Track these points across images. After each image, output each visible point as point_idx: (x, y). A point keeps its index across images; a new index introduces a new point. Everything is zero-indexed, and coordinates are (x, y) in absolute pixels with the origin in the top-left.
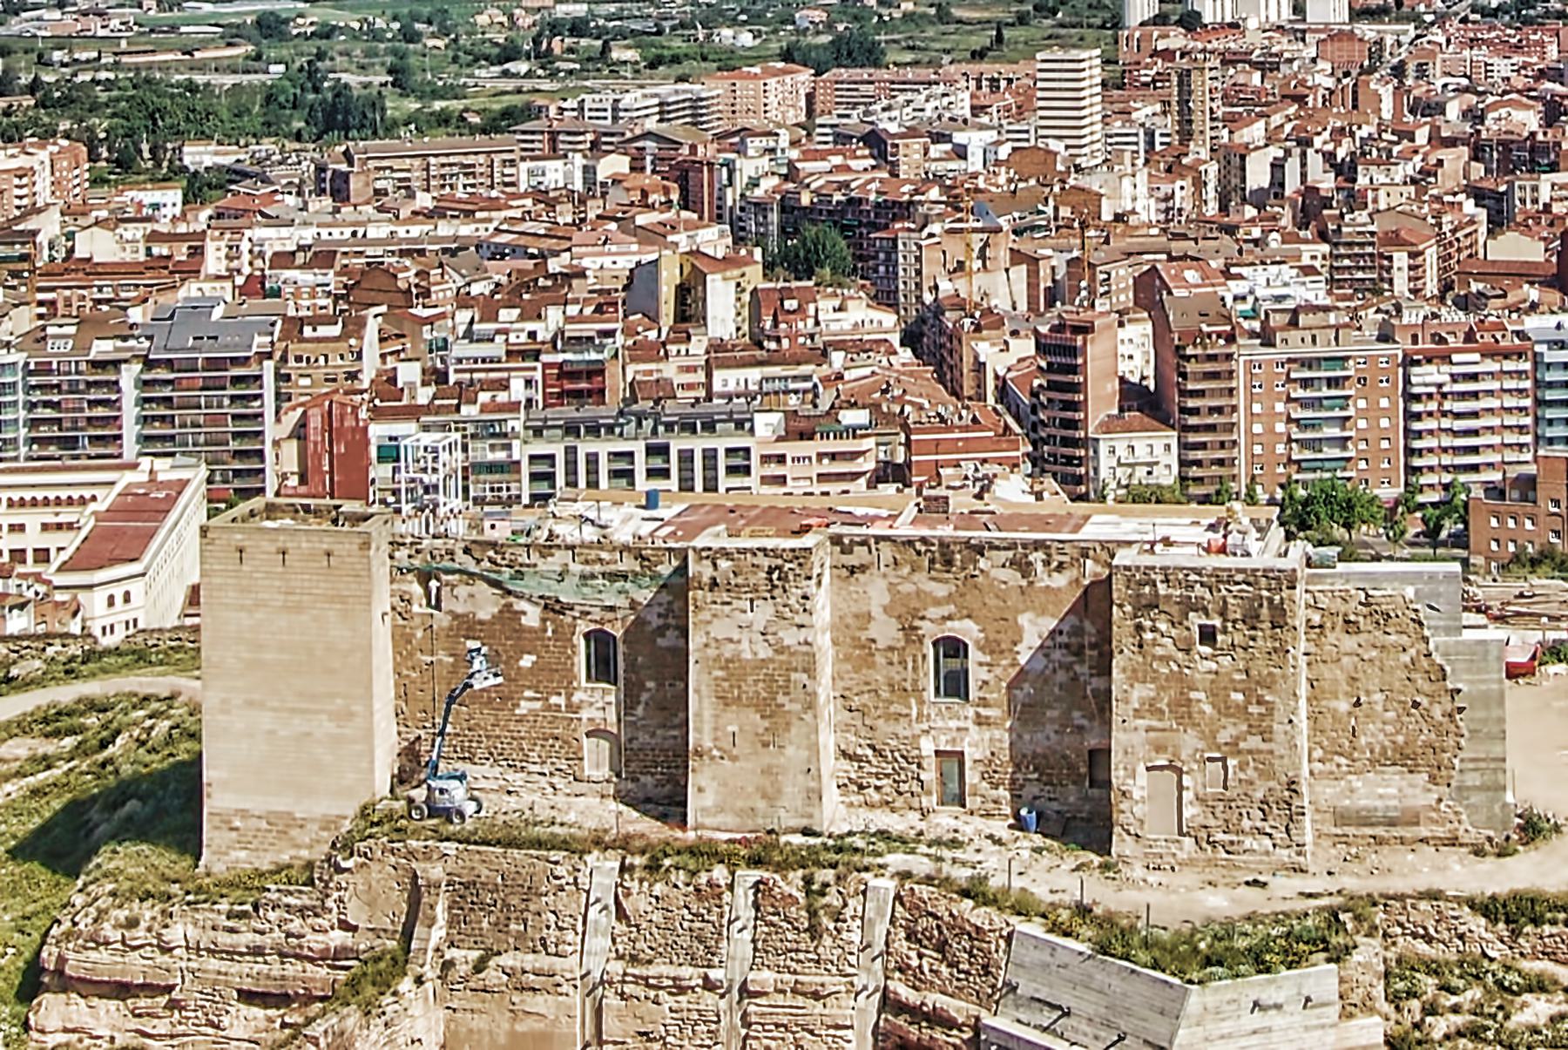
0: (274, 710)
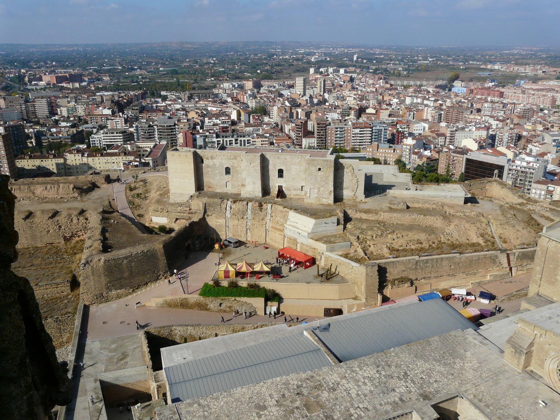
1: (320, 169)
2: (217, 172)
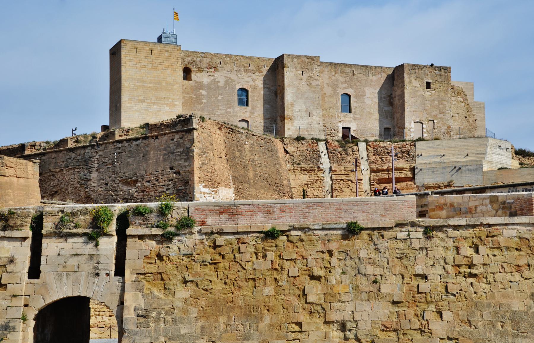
0: (148, 103)
1: (428, 85)
2: (220, 97)
